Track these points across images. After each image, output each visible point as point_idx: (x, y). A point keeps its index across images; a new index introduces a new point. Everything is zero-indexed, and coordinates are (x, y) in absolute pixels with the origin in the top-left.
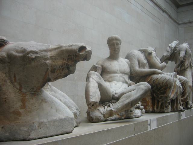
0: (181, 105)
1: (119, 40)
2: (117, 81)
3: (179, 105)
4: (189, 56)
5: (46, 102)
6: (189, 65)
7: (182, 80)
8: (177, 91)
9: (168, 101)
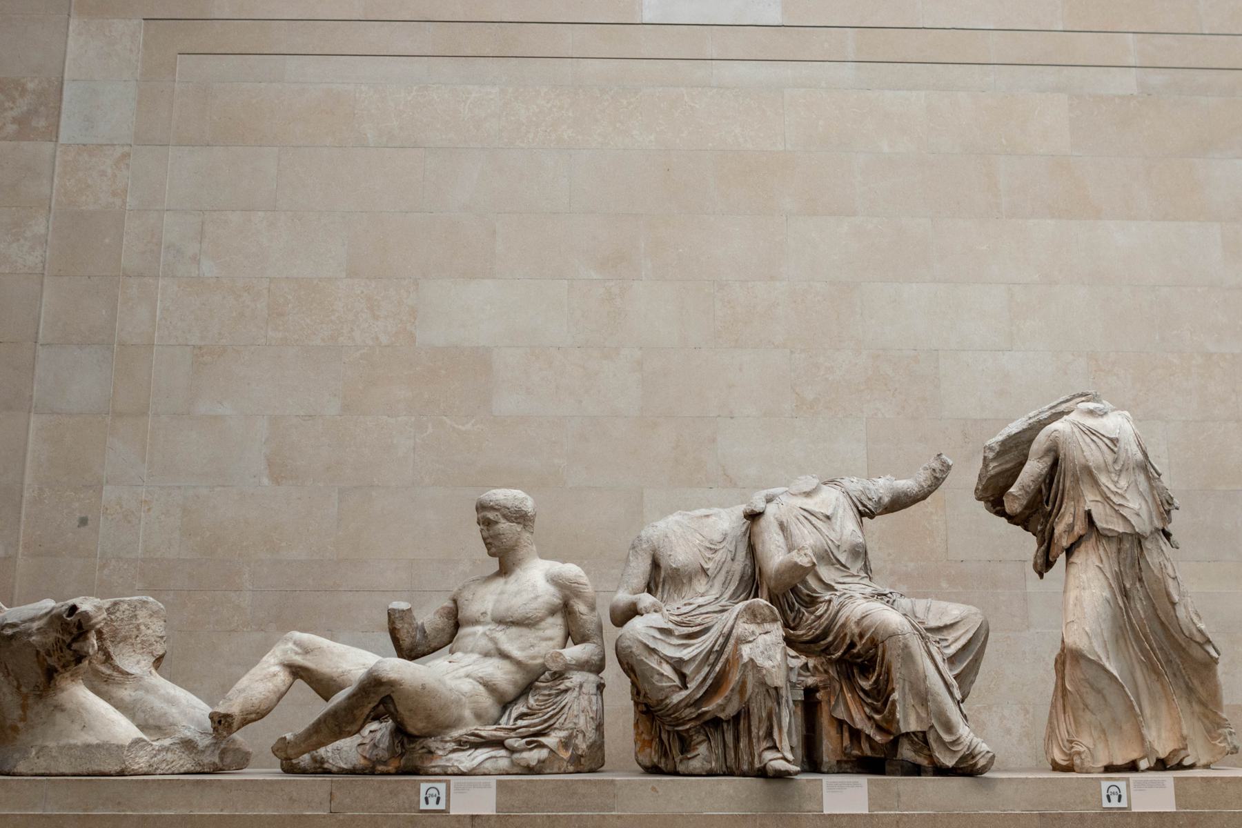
0: (774, 748)
1: (492, 508)
2: (466, 652)
3: (765, 744)
4: (1077, 481)
5: (63, 710)
6: (1079, 528)
7: (869, 628)
8: (743, 685)
9: (683, 724)
